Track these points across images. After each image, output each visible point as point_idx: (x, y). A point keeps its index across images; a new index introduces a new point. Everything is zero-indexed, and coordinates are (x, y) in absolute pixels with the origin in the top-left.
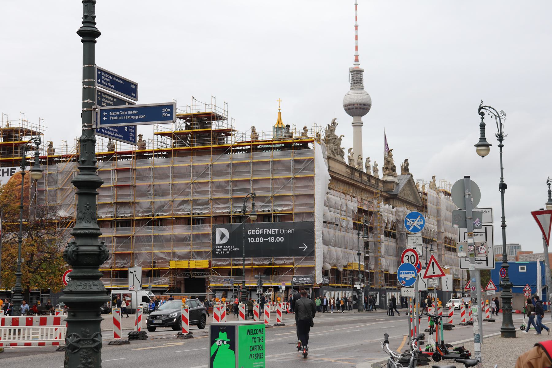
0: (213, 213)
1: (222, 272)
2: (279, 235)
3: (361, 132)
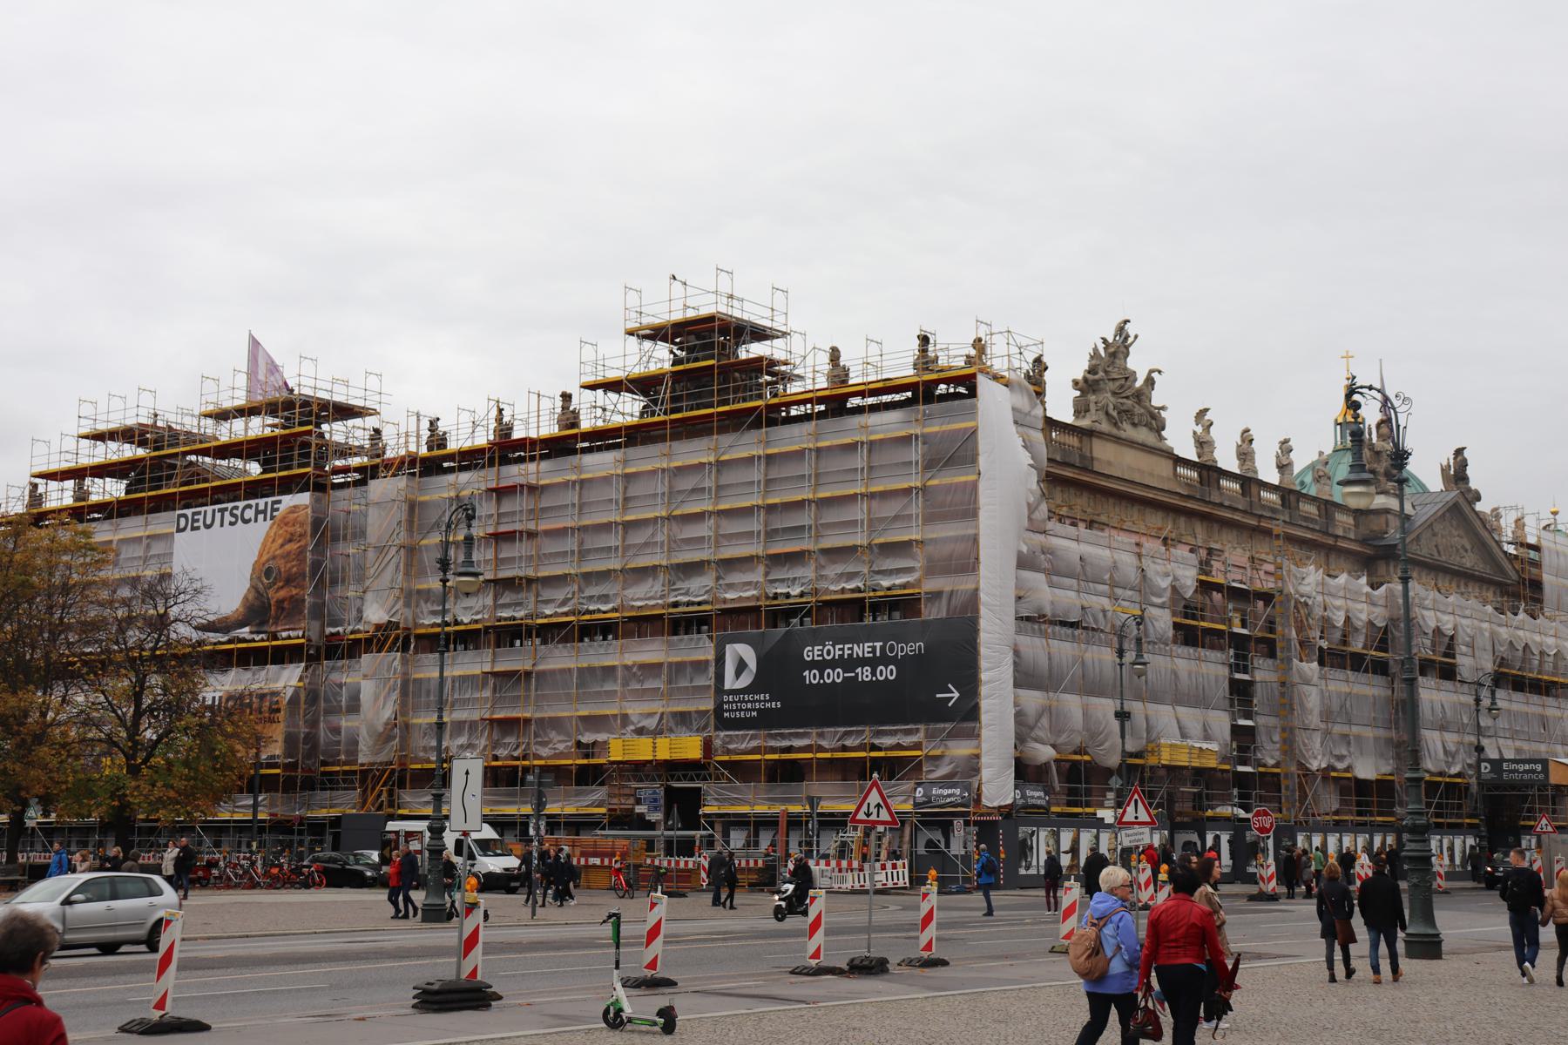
1: (742, 771)
2: (885, 660)
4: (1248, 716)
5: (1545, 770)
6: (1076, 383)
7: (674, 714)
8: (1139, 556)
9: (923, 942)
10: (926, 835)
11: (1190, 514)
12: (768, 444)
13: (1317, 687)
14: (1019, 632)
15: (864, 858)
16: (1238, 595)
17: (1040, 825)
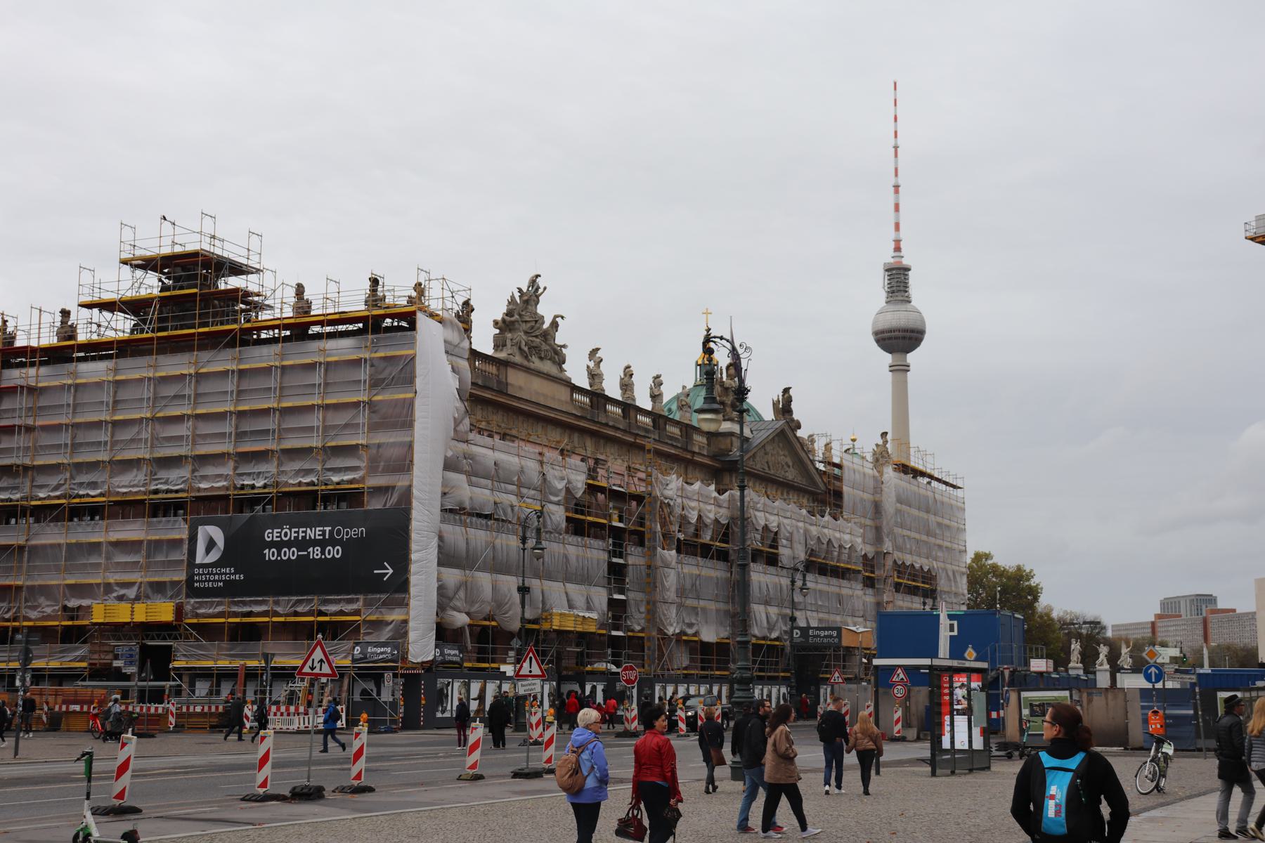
0: (191, 489)
1: (208, 632)
2: (333, 542)
3: (906, 382)
4: (621, 592)
5: (839, 636)
6: (496, 323)
7: (151, 584)
8: (541, 463)
9: (354, 773)
10: (363, 685)
11: (583, 431)
12: (240, 361)
13: (676, 570)
14: (442, 521)
15: (309, 704)
16: (615, 495)
17: (454, 677)
